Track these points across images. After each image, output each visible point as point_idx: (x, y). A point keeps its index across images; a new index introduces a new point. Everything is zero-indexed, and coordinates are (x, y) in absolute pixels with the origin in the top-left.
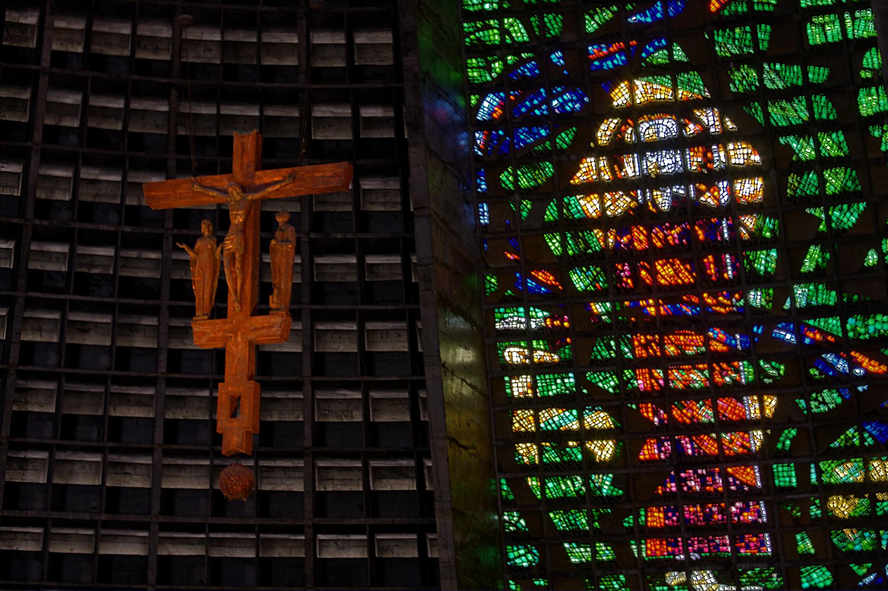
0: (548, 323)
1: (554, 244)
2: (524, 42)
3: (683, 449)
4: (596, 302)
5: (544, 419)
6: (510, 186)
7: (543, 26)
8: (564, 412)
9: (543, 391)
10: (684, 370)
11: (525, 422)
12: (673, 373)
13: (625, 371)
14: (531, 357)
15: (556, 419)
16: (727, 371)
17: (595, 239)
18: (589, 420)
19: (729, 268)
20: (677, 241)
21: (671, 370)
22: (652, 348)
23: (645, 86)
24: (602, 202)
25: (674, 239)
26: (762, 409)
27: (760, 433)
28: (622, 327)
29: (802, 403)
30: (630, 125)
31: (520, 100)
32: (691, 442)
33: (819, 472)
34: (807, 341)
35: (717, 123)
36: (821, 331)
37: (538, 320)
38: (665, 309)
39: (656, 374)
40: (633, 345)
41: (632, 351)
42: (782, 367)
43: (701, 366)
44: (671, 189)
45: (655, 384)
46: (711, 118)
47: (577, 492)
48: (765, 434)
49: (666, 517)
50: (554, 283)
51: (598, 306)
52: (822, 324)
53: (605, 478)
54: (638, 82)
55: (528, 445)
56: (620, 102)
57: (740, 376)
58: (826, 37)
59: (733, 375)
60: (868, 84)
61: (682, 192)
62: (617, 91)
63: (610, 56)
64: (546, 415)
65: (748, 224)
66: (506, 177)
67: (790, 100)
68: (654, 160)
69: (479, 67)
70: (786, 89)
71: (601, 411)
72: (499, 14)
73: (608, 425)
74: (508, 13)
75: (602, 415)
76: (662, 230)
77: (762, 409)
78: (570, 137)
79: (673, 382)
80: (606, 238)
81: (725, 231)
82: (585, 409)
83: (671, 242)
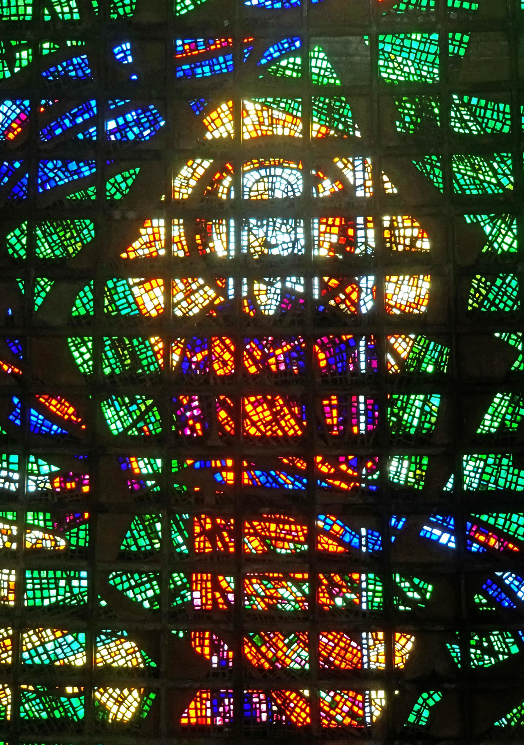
0: (57, 485)
1: (82, 354)
3: (254, 711)
4: (140, 455)
6: (22, 252)
8: (64, 635)
9: (34, 598)
10: (270, 580)
12: (251, 584)
13: (175, 575)
14: (19, 539)
15: (50, 646)
16: (340, 587)
17: (150, 353)
18: (104, 652)
19: (362, 418)
20: (282, 367)
21: (250, 578)
22: (222, 539)
23: (260, 114)
24: (168, 292)
25: (278, 363)
26: (390, 654)
27: (382, 694)
28: (176, 500)
30: (228, 172)
32: (269, 701)
34: (475, 547)
35: (369, 183)
36: (500, 534)
37: (41, 478)
38: (251, 478)
39: (224, 584)
40: (191, 531)
41: (190, 542)
42: (430, 588)
43: (299, 576)
44: (283, 281)
45: (221, 600)
46: (359, 175)
48: (390, 696)
50: (73, 417)
51: (141, 464)
52: (501, 521)
54: (249, 105)
56: (217, 135)
57: (360, 598)
59: (348, 596)
61: (300, 289)
62: (214, 115)
64: (34, 638)
65: (400, 350)
66: (17, 238)
67: (488, 157)
68: (261, 233)
70: (483, 136)
71: (127, 639)
73: (135, 663)
75: (127, 645)
76: (261, 348)
77: (390, 654)
78: (130, 182)
79: (249, 600)
80: (167, 352)
81: (363, 357)
83: (273, 367)
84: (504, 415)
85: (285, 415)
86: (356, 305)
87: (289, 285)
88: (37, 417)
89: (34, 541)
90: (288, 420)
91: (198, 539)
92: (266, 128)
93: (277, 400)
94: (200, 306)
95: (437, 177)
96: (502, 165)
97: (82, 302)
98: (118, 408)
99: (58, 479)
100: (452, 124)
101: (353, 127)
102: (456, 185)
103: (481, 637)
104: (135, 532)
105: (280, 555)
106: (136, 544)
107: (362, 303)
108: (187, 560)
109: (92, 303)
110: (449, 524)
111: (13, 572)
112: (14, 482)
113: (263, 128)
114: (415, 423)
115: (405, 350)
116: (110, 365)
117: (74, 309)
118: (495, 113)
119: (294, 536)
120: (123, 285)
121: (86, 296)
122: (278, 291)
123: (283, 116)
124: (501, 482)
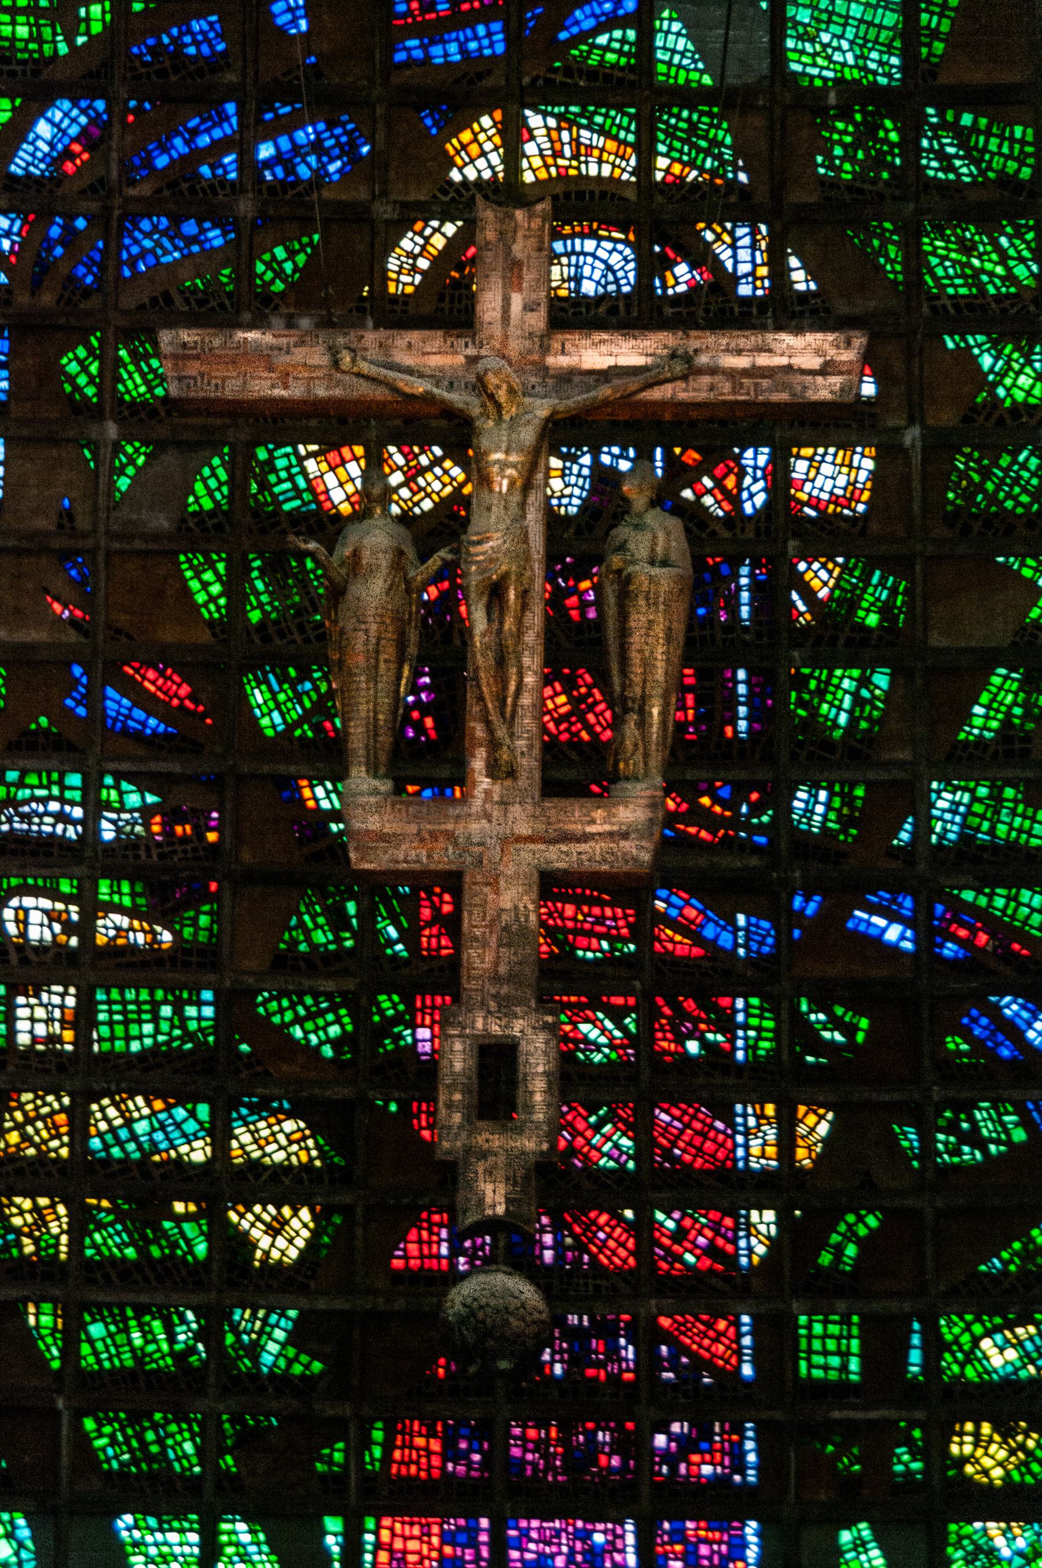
0: (156, 828)
1: (205, 585)
5: (103, 1126)
6: (90, 391)
8: (168, 1108)
9: (112, 1039)
11: (40, 1131)
13: (382, 998)
14: (85, 928)
15: (141, 1127)
16: (696, 1021)
18: (246, 1138)
19: (742, 710)
26: (787, 1143)
27: (769, 1215)
29: (910, 1138)
33: (935, 1347)
35: (763, 271)
37: (126, 816)
40: (414, 916)
42: (864, 1023)
43: (619, 1001)
44: (596, 454)
46: (744, 255)
47: (182, 1358)
49: (450, 1453)
50: (187, 703)
51: (320, 792)
52: (999, 902)
53: (273, 1318)
54: (535, 120)
55: (43, 1201)
56: (471, 173)
57: (732, 1040)
59: (710, 1036)
62: (466, 136)
64: (112, 1112)
65: (816, 584)
66: (80, 362)
67: (989, 225)
71: (290, 1115)
73: (304, 1158)
75: (289, 1126)
77: (787, 1143)
78: (301, 259)
81: (745, 596)
82: (236, 1105)
84: (1010, 708)
85: (596, 703)
86: (734, 499)
87: (606, 459)
88: (119, 703)
89: (112, 933)
90: (602, 713)
91: (427, 932)
92: (566, 163)
93: (581, 676)
94: (435, 497)
95: (893, 262)
96: (1017, 242)
97: (207, 487)
98: (276, 687)
99: (158, 819)
100: (924, 162)
101: (734, 164)
102: (928, 278)
103: (956, 1114)
104: (306, 918)
105: (584, 960)
106: (308, 940)
107: (745, 495)
108: (405, 971)
109: (225, 490)
110: (901, 906)
111: (72, 990)
112: (74, 822)
113: (561, 162)
114: (843, 719)
115: (825, 584)
116: (261, 605)
117: (191, 499)
118: (1006, 144)
119: (609, 928)
120: (287, 455)
121: (214, 474)
122: (586, 472)
123: (599, 141)
124: (1002, 830)
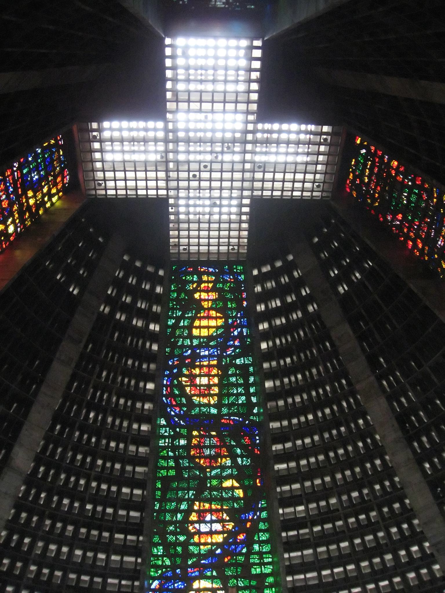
2: (169, 565)
7: (175, 561)
31: (165, 583)
58: (256, 572)
60: (267, 587)
63: (194, 572)
69: (154, 571)
72: (163, 556)
74: (165, 556)
